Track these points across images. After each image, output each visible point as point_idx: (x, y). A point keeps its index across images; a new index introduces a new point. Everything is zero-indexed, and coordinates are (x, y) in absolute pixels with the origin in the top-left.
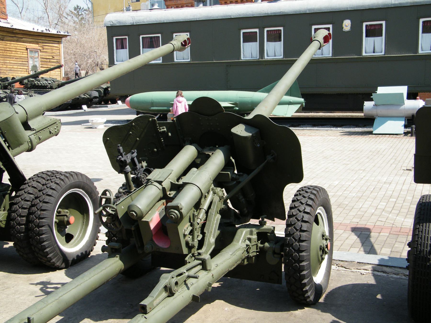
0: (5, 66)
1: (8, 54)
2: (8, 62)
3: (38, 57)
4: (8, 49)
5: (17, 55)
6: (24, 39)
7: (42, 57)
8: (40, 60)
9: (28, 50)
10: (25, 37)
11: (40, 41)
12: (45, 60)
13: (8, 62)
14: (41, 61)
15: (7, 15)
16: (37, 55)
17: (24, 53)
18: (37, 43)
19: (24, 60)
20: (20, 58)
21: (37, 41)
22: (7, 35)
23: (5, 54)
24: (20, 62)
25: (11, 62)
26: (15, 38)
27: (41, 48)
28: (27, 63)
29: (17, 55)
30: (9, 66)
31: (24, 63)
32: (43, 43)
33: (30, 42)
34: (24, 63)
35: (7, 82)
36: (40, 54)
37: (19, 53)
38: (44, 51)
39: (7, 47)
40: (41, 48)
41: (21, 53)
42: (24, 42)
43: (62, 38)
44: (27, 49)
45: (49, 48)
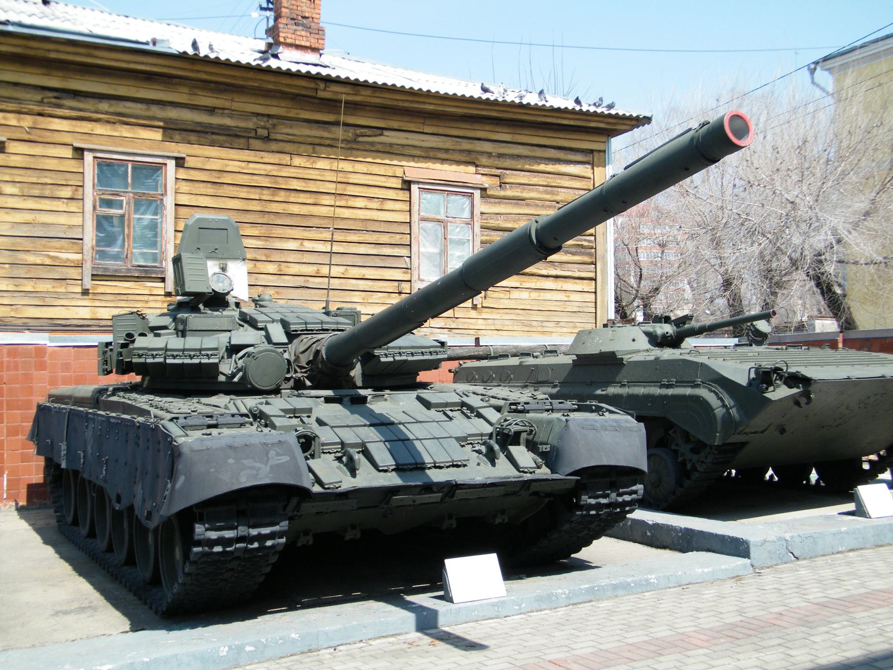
0: (271, 268)
1: (295, 209)
4: (295, 184)
5: (346, 213)
6: (390, 138)
7: (493, 223)
9: (414, 187)
10: (395, 124)
11: (487, 147)
15: (319, 32)
17: (390, 205)
18: (470, 159)
19: (397, 239)
20: (366, 226)
21: (466, 145)
22: (292, 114)
23: (274, 207)
24: (363, 249)
25: (308, 245)
26: (339, 133)
27: (486, 182)
28: (404, 252)
29: (346, 213)
30: (295, 269)
32: (500, 156)
36: (481, 206)
37: (360, 203)
38: (509, 193)
39: (285, 172)
41: (375, 204)
42: (390, 151)
43: (612, 133)
45: (535, 179)
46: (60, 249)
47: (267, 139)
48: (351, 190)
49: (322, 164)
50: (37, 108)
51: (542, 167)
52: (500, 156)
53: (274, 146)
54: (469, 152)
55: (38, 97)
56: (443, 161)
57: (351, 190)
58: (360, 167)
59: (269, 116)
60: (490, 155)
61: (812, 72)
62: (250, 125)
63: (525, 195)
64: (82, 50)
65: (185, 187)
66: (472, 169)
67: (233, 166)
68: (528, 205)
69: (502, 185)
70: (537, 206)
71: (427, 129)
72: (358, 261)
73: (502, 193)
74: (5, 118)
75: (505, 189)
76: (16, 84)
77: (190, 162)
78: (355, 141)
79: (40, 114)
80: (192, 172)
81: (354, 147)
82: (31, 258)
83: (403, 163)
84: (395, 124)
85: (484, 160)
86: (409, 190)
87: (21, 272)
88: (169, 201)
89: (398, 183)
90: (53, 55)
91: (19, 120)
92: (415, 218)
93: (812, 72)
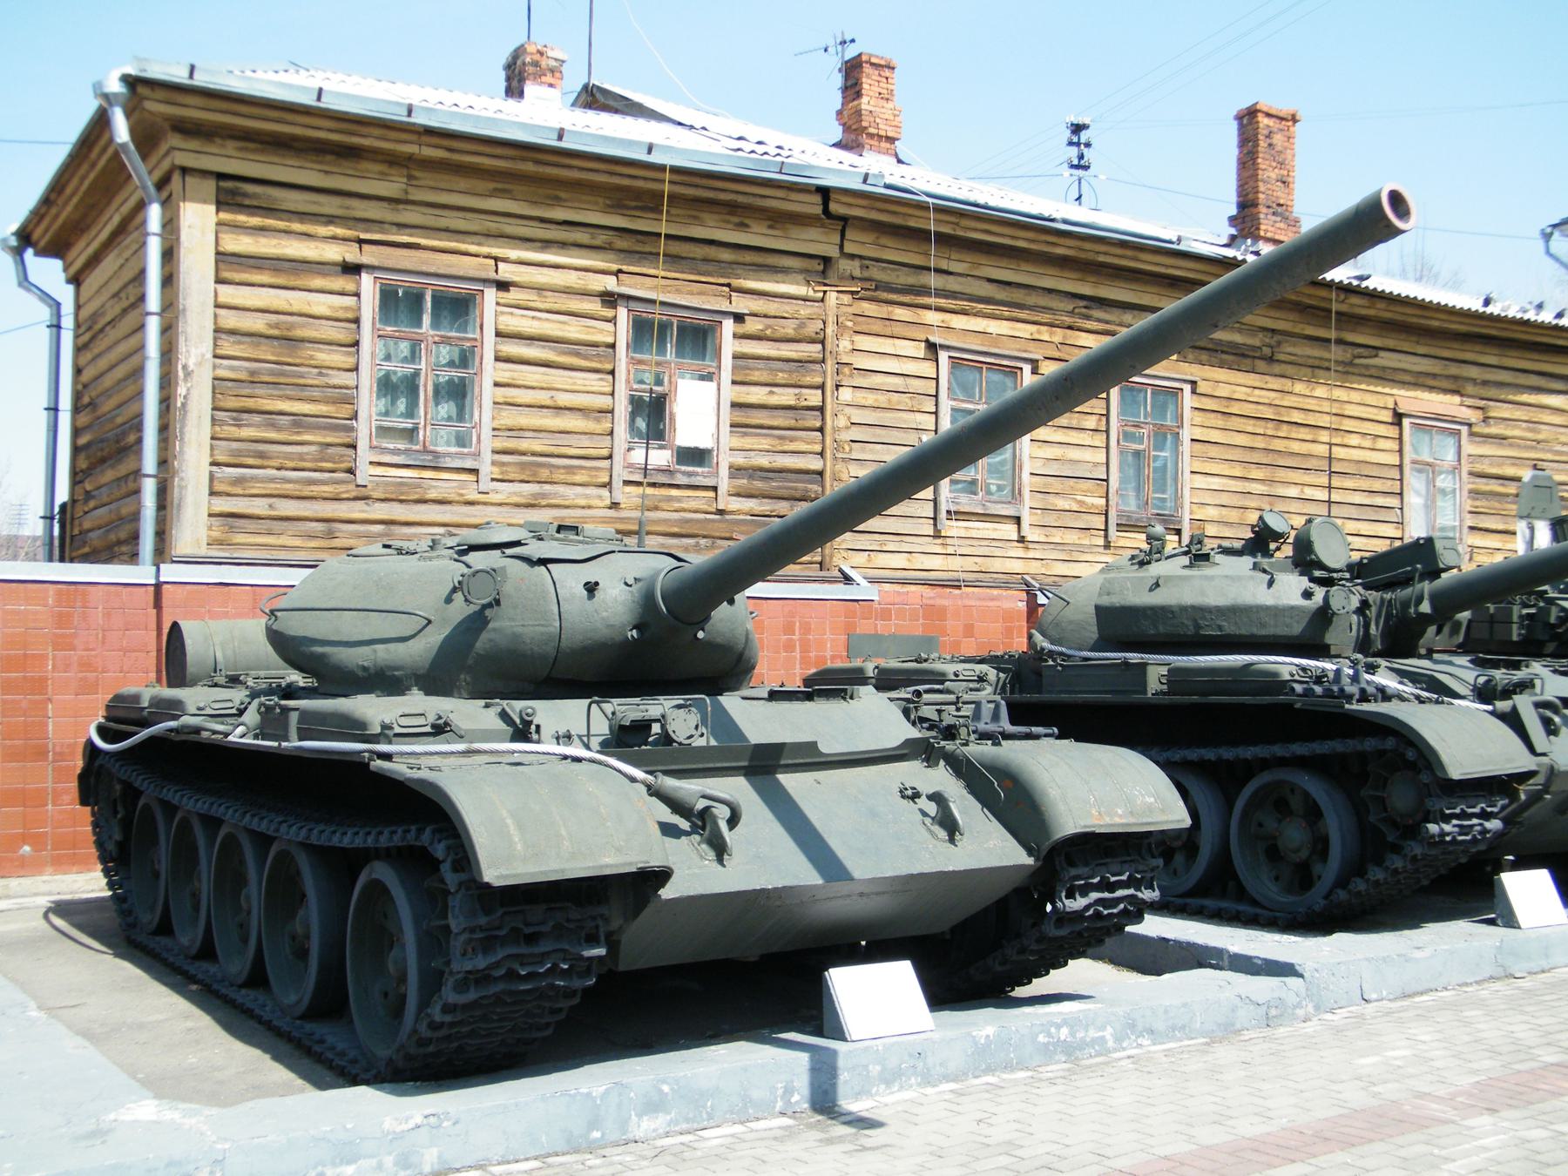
1: (1296, 447)
2: (1293, 492)
3: (1456, 469)
4: (1297, 417)
6: (1386, 359)
7: (1479, 468)
8: (1469, 484)
9: (1406, 422)
10: (1391, 343)
11: (1473, 372)
12: (1494, 486)
13: (1293, 492)
14: (1475, 494)
16: (1450, 456)
17: (1381, 444)
18: (1455, 387)
19: (1377, 485)
21: (1454, 370)
23: (1278, 445)
26: (1336, 353)
28: (1394, 502)
31: (1380, 500)
32: (1485, 383)
33: (1420, 381)
34: (1380, 500)
35: (1427, 587)
36: (1469, 448)
37: (1354, 440)
38: (1493, 430)
39: (1288, 401)
40: (1474, 416)
41: (1367, 443)
42: (1384, 376)
44: (1398, 418)
45: (1518, 413)
46: (1085, 493)
47: (1271, 360)
48: (1348, 425)
49: (1320, 391)
50: (1068, 320)
51: (1525, 398)
52: (1485, 383)
53: (1277, 368)
54: (1455, 378)
55: (1070, 308)
56: (1431, 388)
57: (1348, 425)
58: (1355, 397)
59: (1273, 331)
60: (1474, 381)
61: (1547, 237)
62: (1256, 342)
63: (1509, 433)
64: (1129, 253)
65: (1199, 418)
66: (1457, 399)
67: (1240, 393)
68: (1511, 445)
69: (1486, 419)
70: (1519, 446)
71: (1421, 350)
72: (1354, 512)
73: (1487, 430)
74: (1039, 332)
75: (1489, 425)
76: (1050, 291)
77: (1203, 387)
78: (1351, 364)
79: (1070, 328)
80: (1204, 399)
81: (1350, 371)
82: (1062, 503)
83: (1395, 391)
84: (1391, 343)
85: (1470, 389)
86: (1399, 424)
87: (1051, 519)
88: (1186, 434)
89: (1387, 416)
90: (1101, 258)
91: (1051, 334)
92: (1407, 461)
93: (1547, 237)
